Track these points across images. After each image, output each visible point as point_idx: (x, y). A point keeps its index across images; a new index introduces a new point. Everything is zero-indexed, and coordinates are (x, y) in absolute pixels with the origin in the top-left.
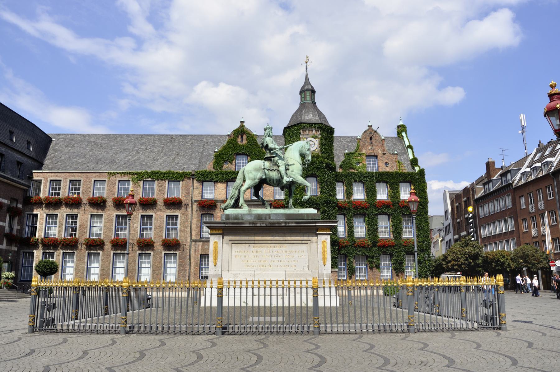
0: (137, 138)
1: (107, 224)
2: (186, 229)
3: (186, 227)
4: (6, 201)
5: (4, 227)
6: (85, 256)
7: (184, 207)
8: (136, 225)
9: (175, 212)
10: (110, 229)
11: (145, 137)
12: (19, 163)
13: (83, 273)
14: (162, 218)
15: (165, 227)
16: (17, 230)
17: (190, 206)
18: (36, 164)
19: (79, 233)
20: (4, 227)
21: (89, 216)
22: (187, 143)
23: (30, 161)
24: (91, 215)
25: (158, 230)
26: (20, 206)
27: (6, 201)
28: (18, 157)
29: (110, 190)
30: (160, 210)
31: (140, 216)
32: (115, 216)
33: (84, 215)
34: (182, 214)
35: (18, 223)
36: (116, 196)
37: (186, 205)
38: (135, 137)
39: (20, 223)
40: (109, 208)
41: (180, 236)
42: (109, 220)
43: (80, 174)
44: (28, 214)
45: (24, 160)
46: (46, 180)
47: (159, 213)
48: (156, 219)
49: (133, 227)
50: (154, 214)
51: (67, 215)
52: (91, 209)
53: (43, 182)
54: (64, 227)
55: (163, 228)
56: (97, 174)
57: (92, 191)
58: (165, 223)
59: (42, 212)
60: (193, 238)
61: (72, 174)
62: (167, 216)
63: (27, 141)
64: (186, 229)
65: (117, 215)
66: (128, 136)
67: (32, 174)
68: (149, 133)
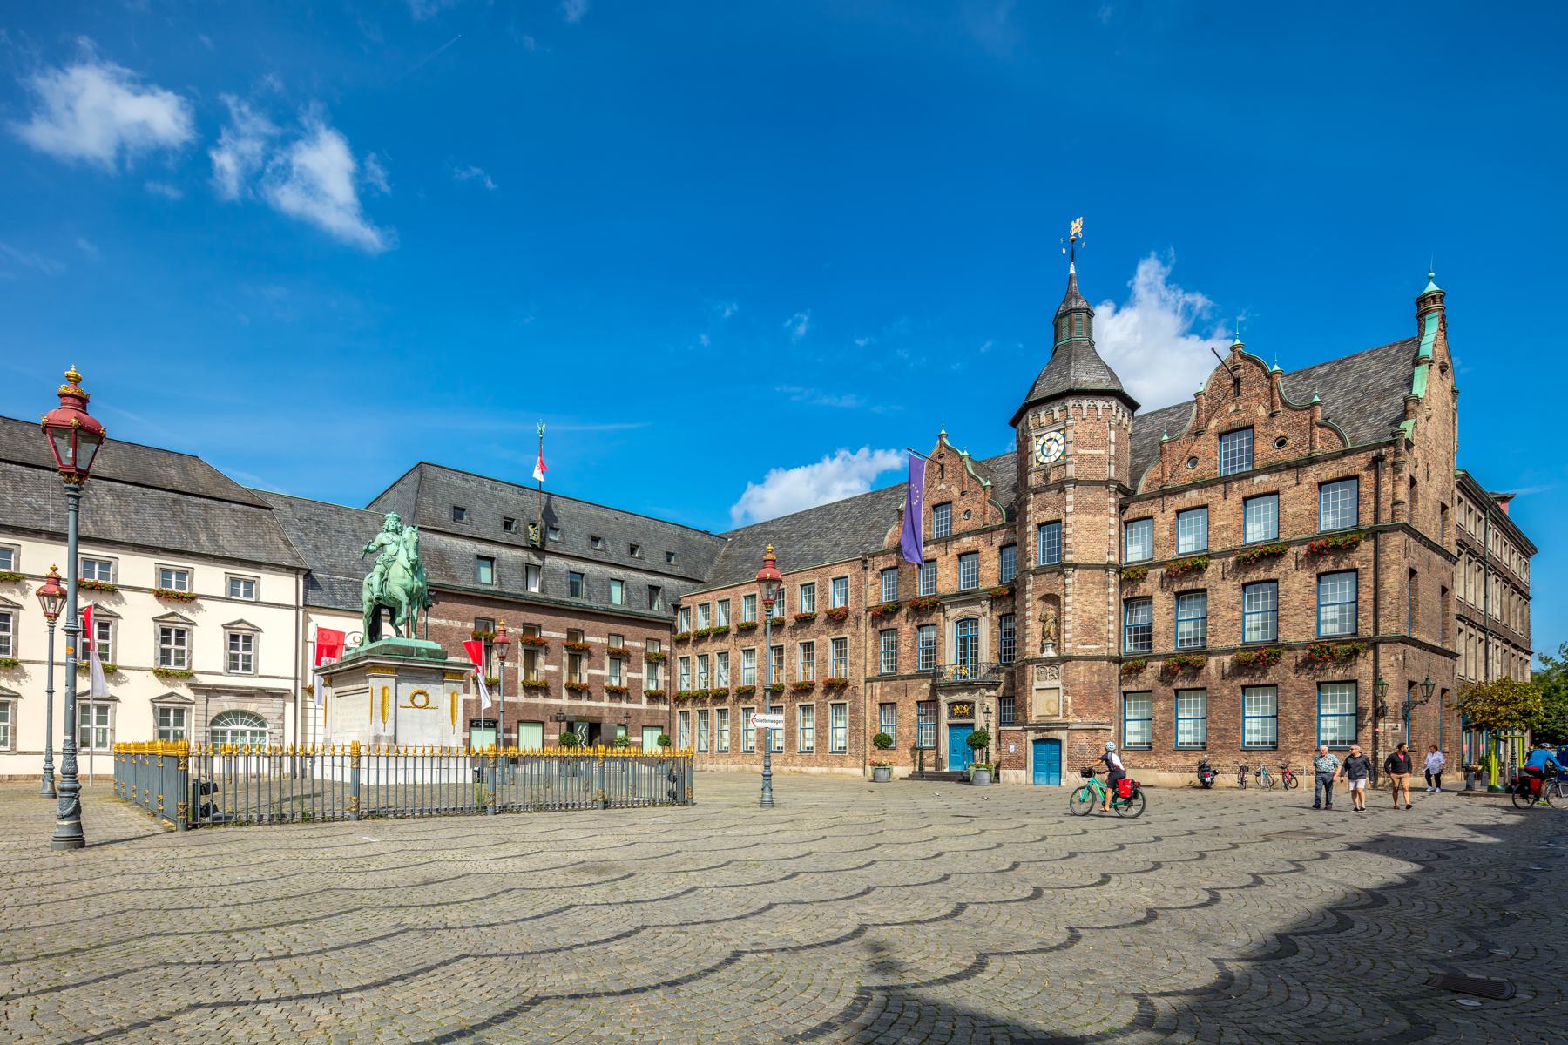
3: (858, 656)
12: (654, 589)
14: (825, 645)
23: (676, 582)
26: (666, 648)
39: (670, 672)
42: (763, 656)
45: (665, 582)
66: (820, 508)
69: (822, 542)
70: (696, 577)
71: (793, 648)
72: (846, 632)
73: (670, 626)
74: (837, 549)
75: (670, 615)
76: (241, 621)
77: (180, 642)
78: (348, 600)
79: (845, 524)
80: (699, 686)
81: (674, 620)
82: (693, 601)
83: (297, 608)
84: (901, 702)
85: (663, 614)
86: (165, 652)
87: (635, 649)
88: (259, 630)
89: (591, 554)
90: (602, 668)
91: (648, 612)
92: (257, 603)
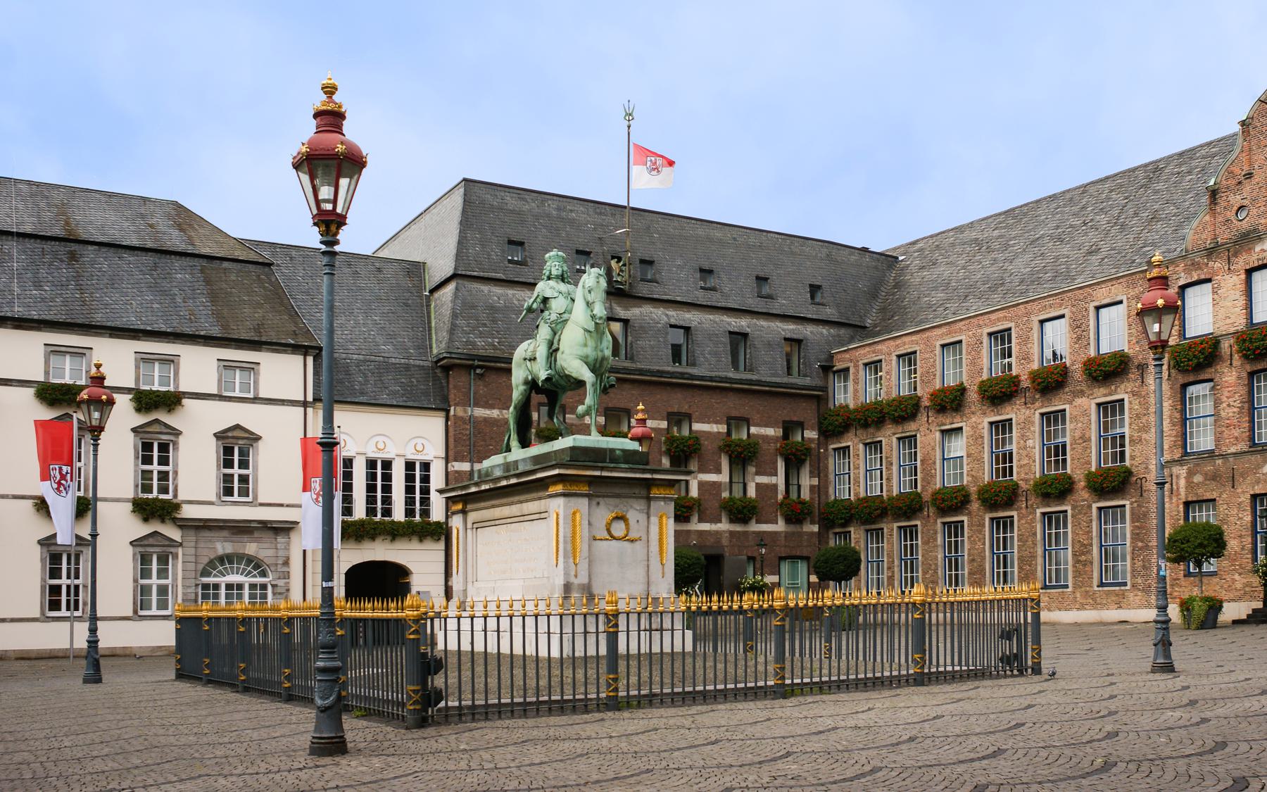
0: (1071, 199)
1: (973, 450)
2: (1144, 436)
3: (1145, 429)
4: (770, 432)
5: (775, 486)
6: (936, 533)
7: (1133, 374)
8: (1030, 443)
9: (1116, 392)
10: (980, 460)
11: (1092, 190)
13: (936, 571)
14: (1086, 413)
15: (1093, 439)
16: (812, 487)
17: (1151, 368)
18: (843, 331)
19: (923, 479)
20: (775, 486)
21: (938, 435)
22: (1189, 173)
23: (824, 330)
24: (943, 432)
25: (1079, 448)
27: (770, 432)
28: (790, 329)
29: (973, 363)
30: (1082, 393)
31: (1037, 416)
32: (986, 425)
33: (927, 432)
34: (1134, 394)
35: (811, 472)
36: (985, 376)
37: (1142, 368)
38: (1068, 196)
40: (973, 409)
41: (1133, 458)
42: (978, 438)
43: (914, 338)
44: (835, 450)
45: (807, 331)
46: (856, 366)
47: (1079, 401)
48: (1074, 419)
49: (1025, 448)
50: (1067, 407)
51: (899, 439)
52: (941, 418)
53: (852, 370)
54: (895, 468)
55: (1090, 439)
56: (944, 330)
57: (938, 374)
58: (1094, 426)
59: (856, 440)
60: (1167, 457)
61: (899, 341)
62: (1099, 405)
63: (811, 286)
64: (1144, 436)
65: (991, 423)
67: (831, 357)
68: (1103, 176)
69: (1065, 250)
70: (855, 320)
71: (1028, 422)
72: (1122, 392)
73: (819, 397)
74: (1095, 259)
75: (818, 382)
76: (237, 427)
77: (164, 461)
78: (369, 388)
79: (1103, 219)
80: (897, 486)
81: (824, 389)
82: (856, 355)
83: (305, 404)
84: (1223, 496)
85: (807, 381)
86: (146, 475)
87: (766, 438)
88: (258, 438)
89: (701, 297)
90: (719, 471)
91: (785, 380)
92: (256, 400)
